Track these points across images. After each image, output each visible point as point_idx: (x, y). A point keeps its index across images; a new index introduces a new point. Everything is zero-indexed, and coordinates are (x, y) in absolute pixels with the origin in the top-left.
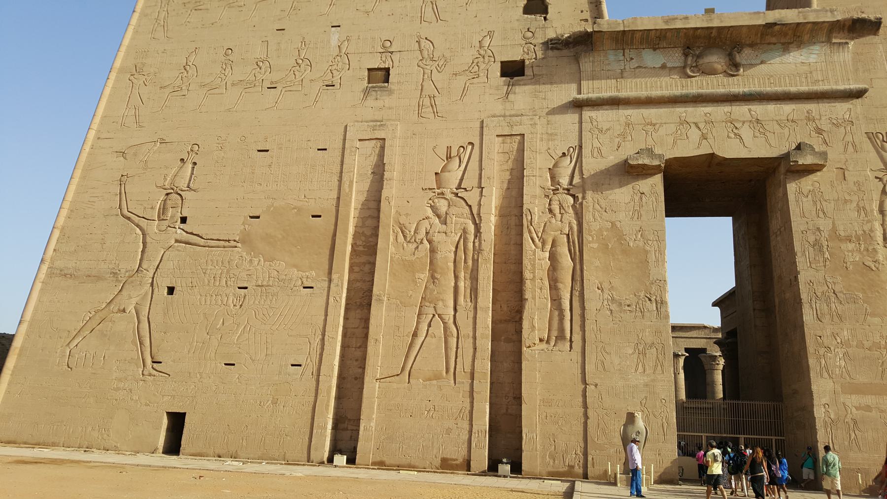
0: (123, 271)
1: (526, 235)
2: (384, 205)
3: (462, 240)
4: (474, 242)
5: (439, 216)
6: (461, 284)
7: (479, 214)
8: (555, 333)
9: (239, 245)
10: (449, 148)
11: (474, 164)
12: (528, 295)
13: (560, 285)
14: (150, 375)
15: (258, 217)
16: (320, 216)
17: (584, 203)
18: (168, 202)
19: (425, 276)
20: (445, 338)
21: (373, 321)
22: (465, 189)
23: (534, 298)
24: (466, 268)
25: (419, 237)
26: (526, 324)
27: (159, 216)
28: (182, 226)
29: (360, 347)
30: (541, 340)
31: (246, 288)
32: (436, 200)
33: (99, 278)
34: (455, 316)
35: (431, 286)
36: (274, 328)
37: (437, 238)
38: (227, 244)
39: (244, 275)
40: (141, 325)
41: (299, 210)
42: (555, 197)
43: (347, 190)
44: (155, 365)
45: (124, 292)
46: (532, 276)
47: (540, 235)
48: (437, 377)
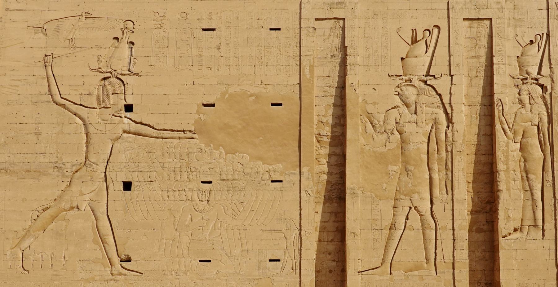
0: (68, 165)
1: (498, 126)
2: (348, 91)
3: (433, 131)
4: (446, 133)
5: (407, 105)
6: (436, 176)
7: (450, 104)
8: (527, 223)
9: (195, 136)
10: (414, 31)
11: (442, 50)
12: (502, 186)
13: (531, 176)
14: (120, 274)
15: (213, 105)
16: (280, 104)
17: (553, 94)
18: (108, 87)
19: (396, 168)
20: (423, 230)
21: (349, 215)
22: (434, 76)
23: (508, 189)
24: (439, 160)
25: (389, 127)
26: (501, 215)
27: (98, 103)
28: (128, 114)
29: (332, 241)
30: (515, 230)
31: (210, 182)
32: (404, 88)
33: (40, 173)
34: (431, 208)
35: (405, 178)
36: (246, 223)
37: (408, 128)
38: (182, 135)
39: (205, 168)
40: (100, 224)
41: (257, 97)
42: (524, 87)
43: (308, 76)
44: (124, 264)
45: (74, 188)
46: (505, 167)
47: (511, 126)
48: (418, 268)
